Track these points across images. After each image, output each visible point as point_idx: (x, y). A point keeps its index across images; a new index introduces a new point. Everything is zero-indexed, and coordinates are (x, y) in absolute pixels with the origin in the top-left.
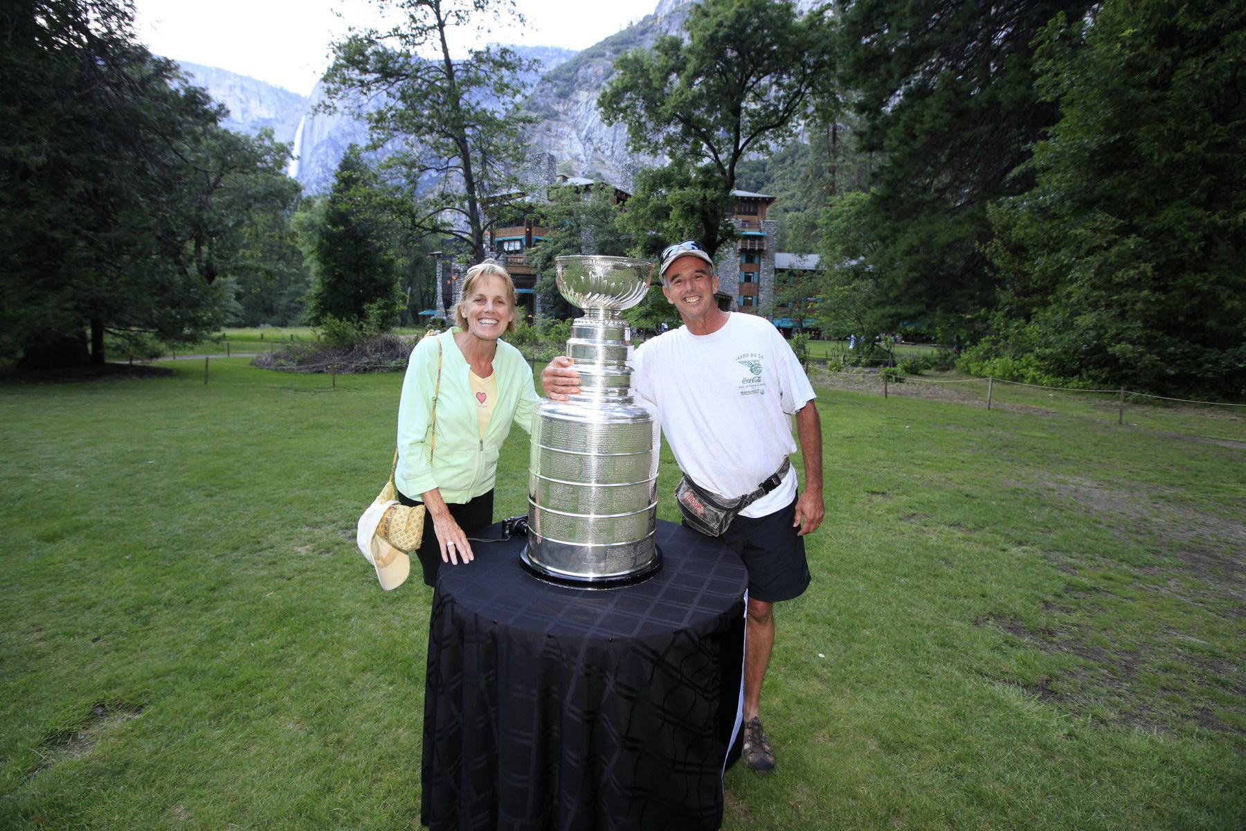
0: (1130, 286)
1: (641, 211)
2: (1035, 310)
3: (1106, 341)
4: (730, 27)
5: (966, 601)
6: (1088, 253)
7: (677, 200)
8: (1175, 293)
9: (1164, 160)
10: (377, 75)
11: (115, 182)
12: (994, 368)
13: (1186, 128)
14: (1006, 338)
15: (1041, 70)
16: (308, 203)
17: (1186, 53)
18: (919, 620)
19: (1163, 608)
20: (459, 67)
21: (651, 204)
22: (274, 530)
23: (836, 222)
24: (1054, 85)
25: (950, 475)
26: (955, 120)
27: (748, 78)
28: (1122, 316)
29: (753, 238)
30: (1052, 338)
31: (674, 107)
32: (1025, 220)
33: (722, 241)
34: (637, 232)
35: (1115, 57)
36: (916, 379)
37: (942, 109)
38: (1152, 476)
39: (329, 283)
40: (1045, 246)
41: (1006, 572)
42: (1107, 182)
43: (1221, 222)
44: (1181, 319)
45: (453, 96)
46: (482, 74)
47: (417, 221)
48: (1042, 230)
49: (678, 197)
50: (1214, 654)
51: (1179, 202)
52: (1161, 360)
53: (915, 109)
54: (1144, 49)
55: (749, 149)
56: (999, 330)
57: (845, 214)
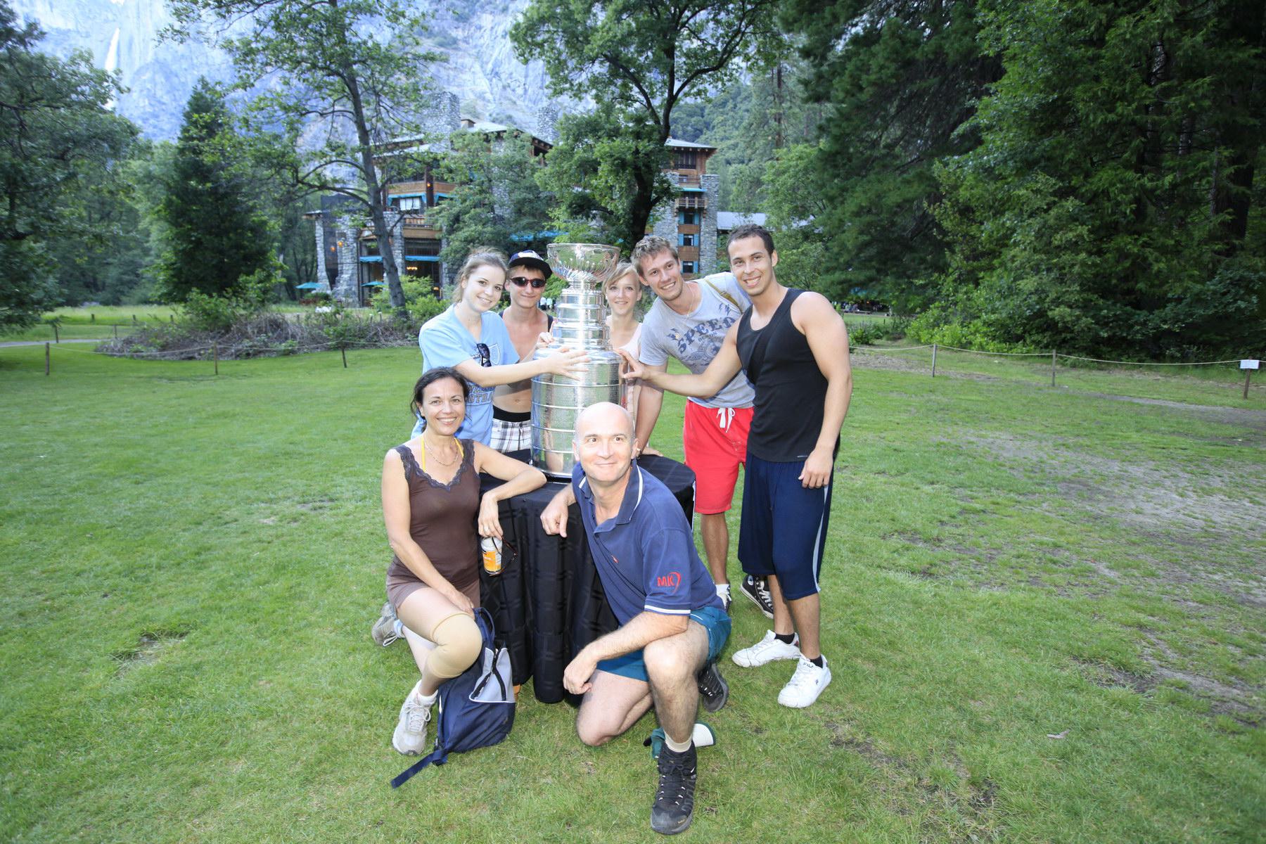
0: (1068, 249)
1: (566, 165)
2: (981, 274)
3: (1046, 305)
6: (1030, 216)
8: (1108, 255)
9: (1099, 120)
12: (944, 336)
13: (1117, 89)
14: (956, 304)
15: (983, 21)
17: (1120, 10)
18: (838, 538)
19: (1032, 521)
21: (576, 157)
22: (230, 507)
23: (782, 178)
24: (996, 39)
25: (883, 435)
27: (682, 12)
28: (1061, 280)
29: (693, 194)
30: (998, 304)
32: (970, 179)
33: (657, 200)
34: (560, 190)
36: (866, 349)
37: (887, 59)
38: (1064, 428)
40: (991, 207)
43: (1149, 185)
44: (1114, 281)
48: (987, 190)
49: (608, 149)
50: (1056, 546)
51: (1112, 163)
52: (1097, 323)
53: (861, 57)
55: (686, 95)
56: (948, 296)
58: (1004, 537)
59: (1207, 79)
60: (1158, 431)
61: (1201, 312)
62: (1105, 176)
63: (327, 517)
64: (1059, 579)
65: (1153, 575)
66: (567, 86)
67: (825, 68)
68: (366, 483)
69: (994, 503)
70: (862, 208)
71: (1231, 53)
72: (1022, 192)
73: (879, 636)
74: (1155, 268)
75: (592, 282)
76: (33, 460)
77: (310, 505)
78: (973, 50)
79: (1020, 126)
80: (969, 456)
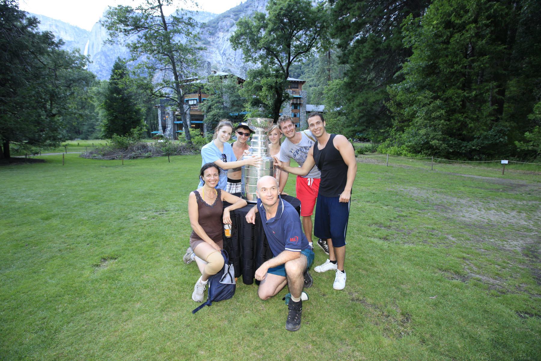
1: (250, 88)
2: (405, 128)
4: (285, 10)
5: (367, 221)
6: (423, 107)
7: (265, 83)
8: (452, 121)
10: (133, 27)
11: (14, 75)
13: (454, 60)
14: (395, 139)
16: (98, 83)
17: (455, 31)
19: (424, 220)
20: (169, 25)
21: (254, 85)
23: (331, 92)
25: (369, 188)
26: (375, 53)
27: (293, 31)
28: (435, 130)
29: (297, 98)
31: (263, 44)
32: (401, 93)
33: (284, 100)
34: (248, 97)
35: (430, 32)
36: (362, 156)
38: (436, 186)
39: (111, 120)
40: (408, 103)
41: (381, 213)
42: (429, 79)
43: (467, 95)
44: (454, 131)
45: (167, 37)
46: (180, 28)
47: (153, 92)
48: (407, 97)
50: (433, 229)
51: (453, 87)
52: (448, 146)
54: (440, 29)
55: (295, 61)
57: (334, 89)
58: (414, 226)
59: (487, 56)
60: (471, 187)
61: (487, 142)
62: (450, 92)
63: (165, 217)
64: (434, 241)
65: (469, 240)
66: (251, 58)
67: (346, 51)
68: (178, 205)
69: (410, 213)
70: (360, 103)
71: (496, 47)
72: (420, 97)
73: (368, 261)
74: (470, 126)
75: (263, 132)
76: (60, 196)
77: (159, 213)
78: (402, 45)
79: (419, 73)
80: (401, 196)
